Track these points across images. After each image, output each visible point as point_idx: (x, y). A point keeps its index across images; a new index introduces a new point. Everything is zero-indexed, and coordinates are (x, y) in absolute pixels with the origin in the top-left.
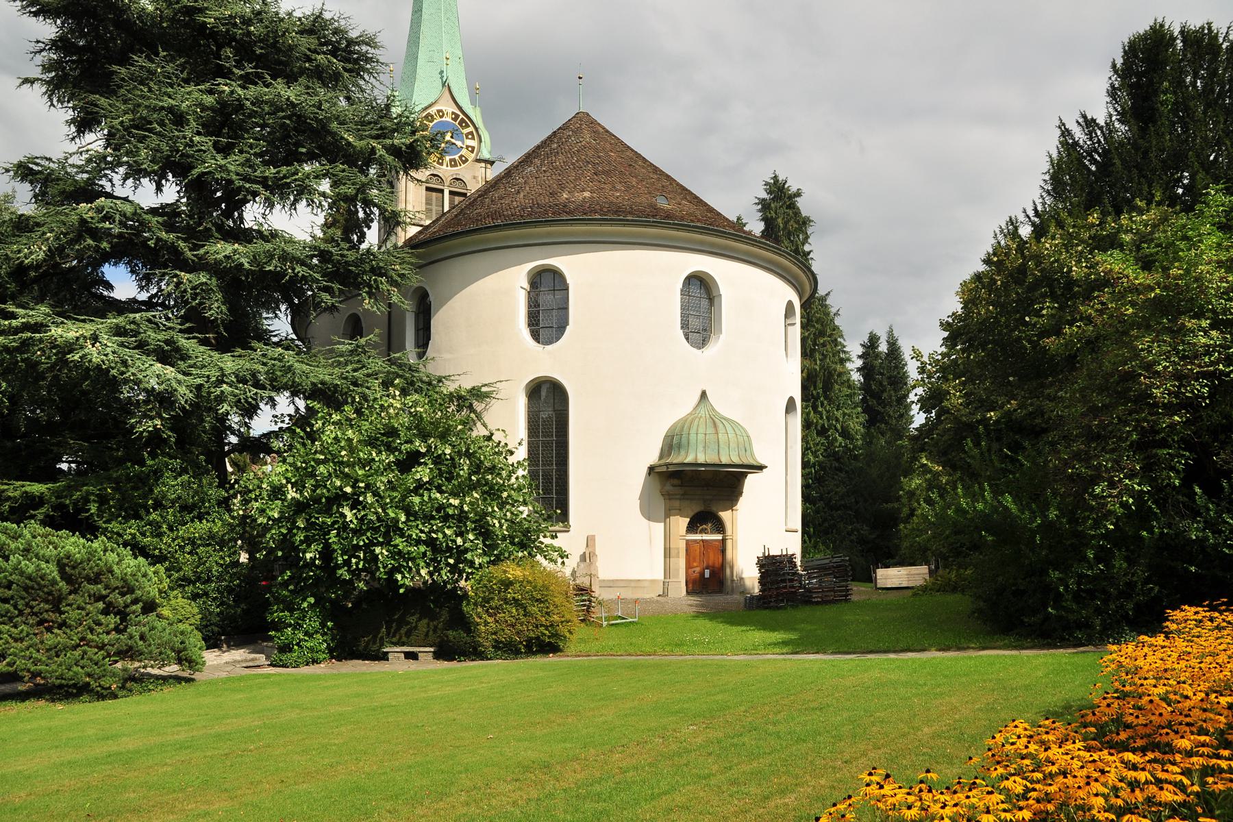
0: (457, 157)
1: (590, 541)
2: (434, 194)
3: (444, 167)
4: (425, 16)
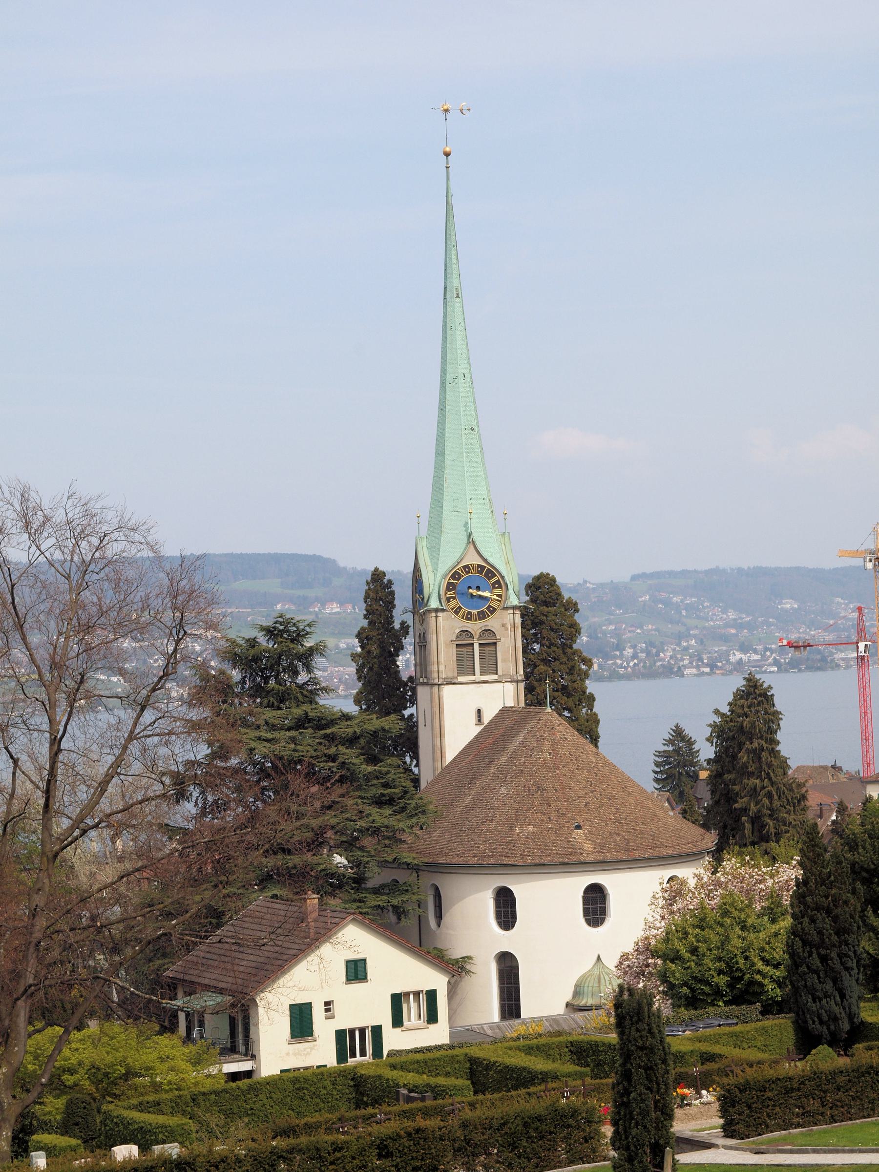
2: (464, 649)
4: (448, 463)
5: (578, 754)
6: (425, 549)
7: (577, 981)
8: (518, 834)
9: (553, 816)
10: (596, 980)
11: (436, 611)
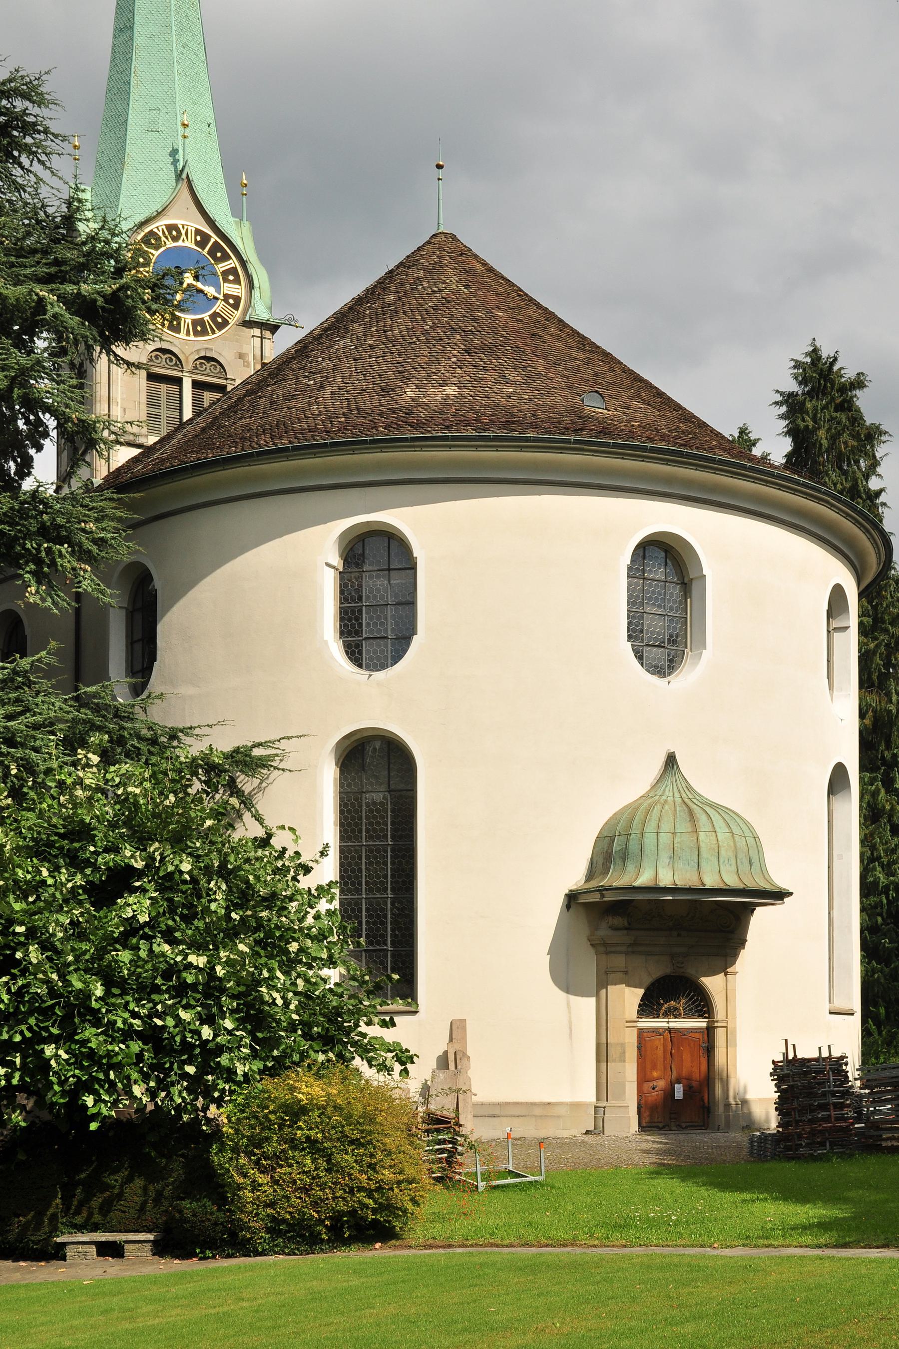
0: (206, 316)
1: (457, 1030)
2: (164, 387)
3: (183, 335)
10: (682, 813)
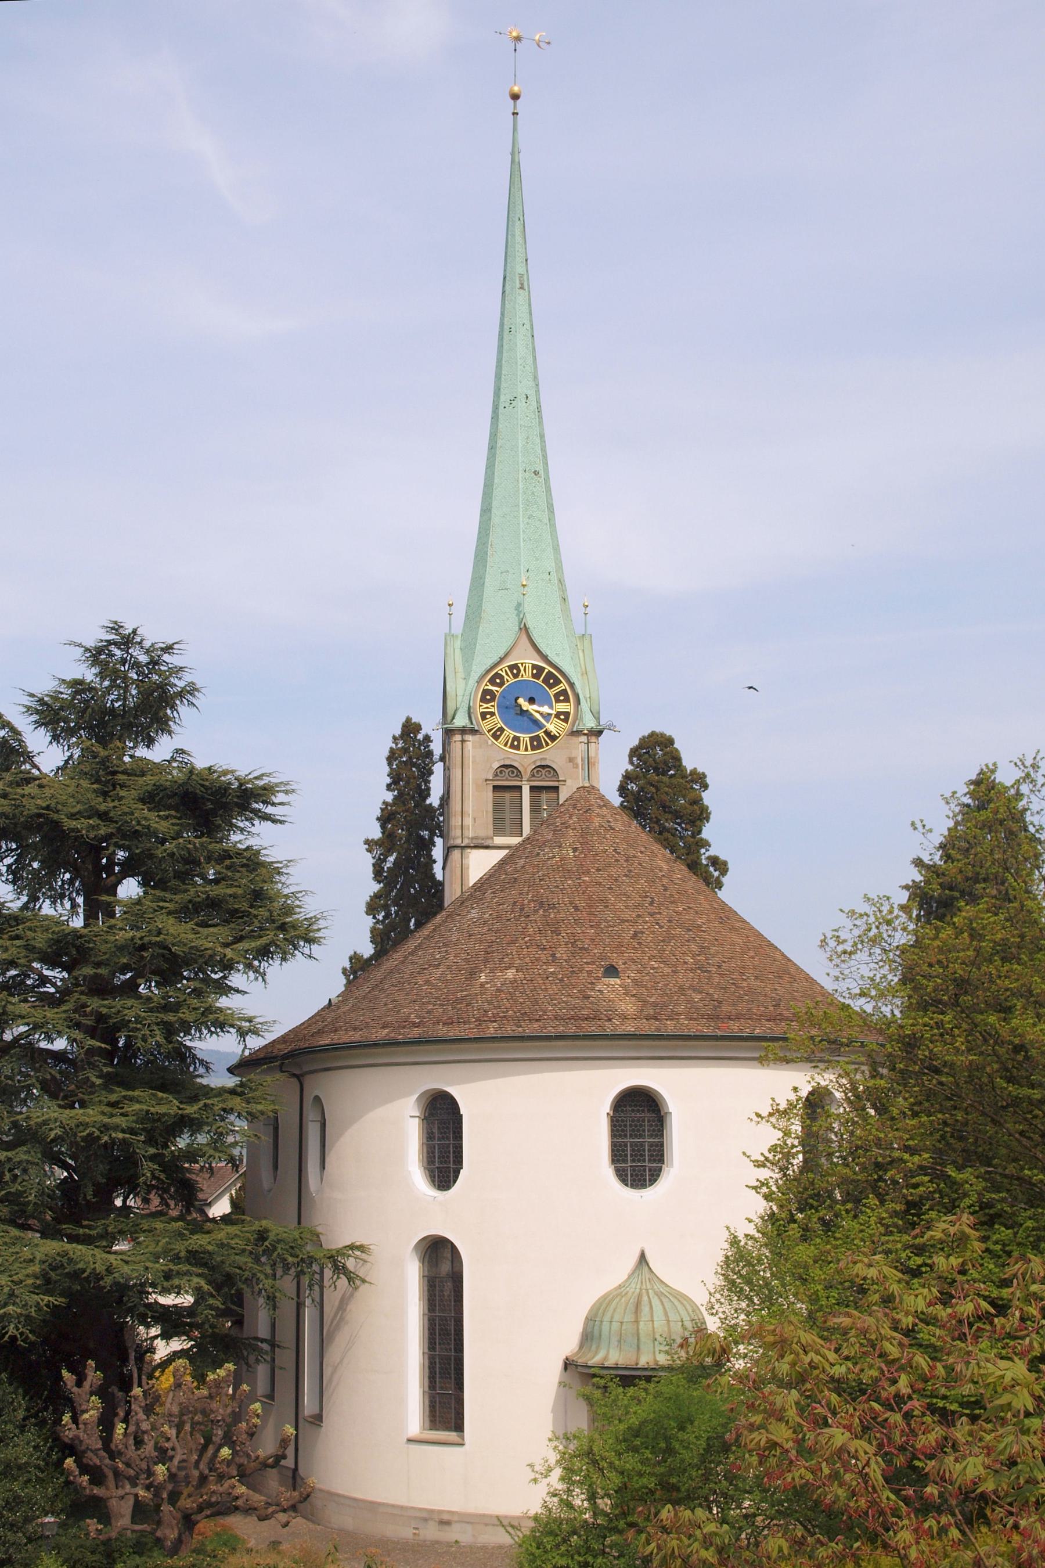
2: (507, 796)
3: (522, 752)
5: (632, 852)
6: (458, 652)
7: (592, 1308)
8: (482, 985)
9: (561, 953)
10: (631, 1307)
11: (463, 731)
